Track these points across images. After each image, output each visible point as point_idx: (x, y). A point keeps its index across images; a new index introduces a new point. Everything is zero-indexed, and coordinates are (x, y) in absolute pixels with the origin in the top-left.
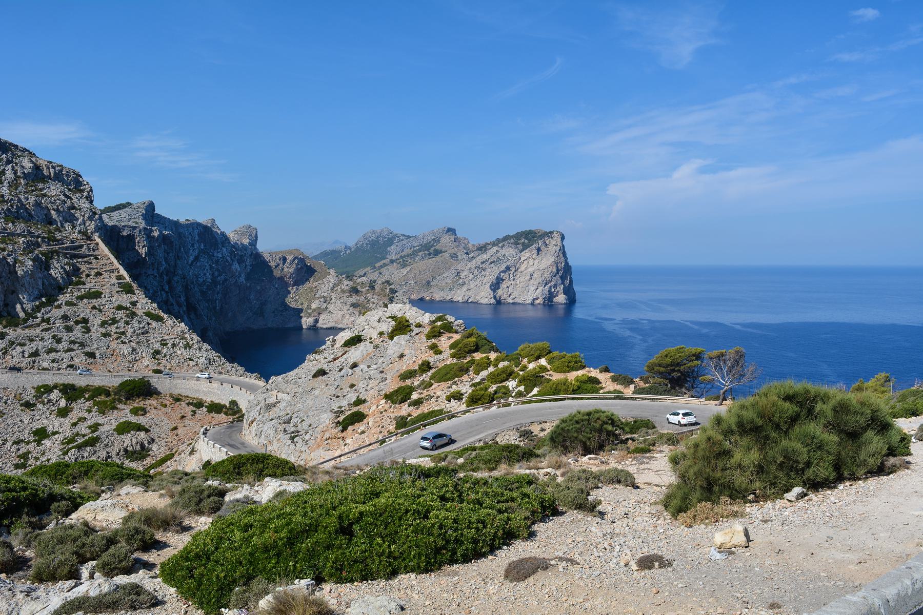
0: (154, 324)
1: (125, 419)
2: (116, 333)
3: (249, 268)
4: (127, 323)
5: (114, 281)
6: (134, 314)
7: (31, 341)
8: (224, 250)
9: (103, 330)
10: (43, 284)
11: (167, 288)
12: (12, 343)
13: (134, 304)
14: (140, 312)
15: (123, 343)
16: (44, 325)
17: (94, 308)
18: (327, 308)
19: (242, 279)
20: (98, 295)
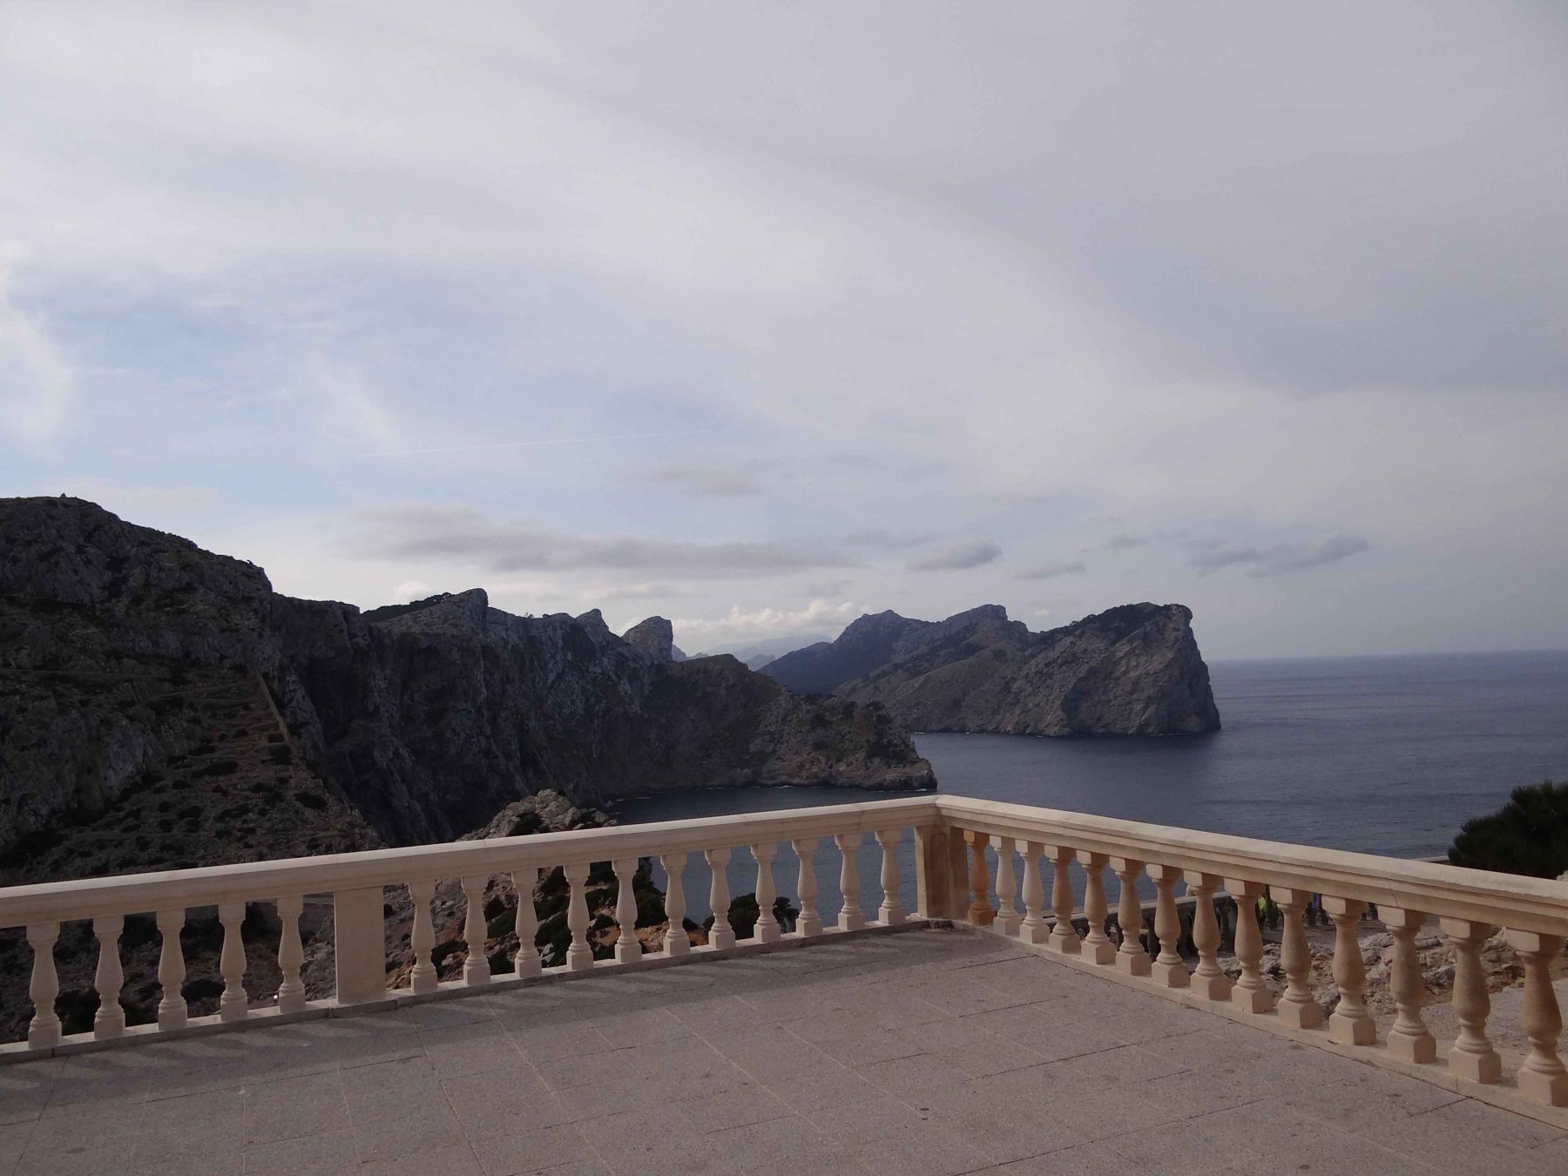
0: (309, 814)
1: (204, 976)
2: (240, 830)
3: (647, 690)
4: (263, 813)
5: (264, 743)
6: (280, 798)
7: (102, 847)
8: (605, 660)
9: (220, 826)
10: (145, 754)
11: (488, 729)
12: (70, 852)
13: (283, 781)
14: (289, 794)
15: (247, 846)
16: (130, 821)
17: (218, 789)
18: (774, 751)
19: (636, 707)
20: (229, 767)
